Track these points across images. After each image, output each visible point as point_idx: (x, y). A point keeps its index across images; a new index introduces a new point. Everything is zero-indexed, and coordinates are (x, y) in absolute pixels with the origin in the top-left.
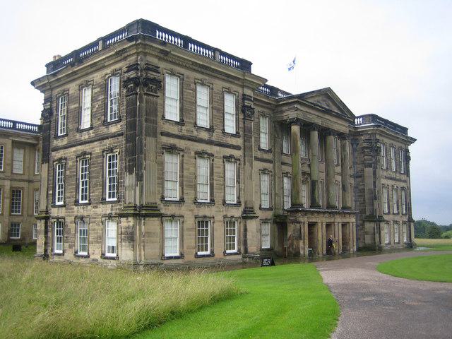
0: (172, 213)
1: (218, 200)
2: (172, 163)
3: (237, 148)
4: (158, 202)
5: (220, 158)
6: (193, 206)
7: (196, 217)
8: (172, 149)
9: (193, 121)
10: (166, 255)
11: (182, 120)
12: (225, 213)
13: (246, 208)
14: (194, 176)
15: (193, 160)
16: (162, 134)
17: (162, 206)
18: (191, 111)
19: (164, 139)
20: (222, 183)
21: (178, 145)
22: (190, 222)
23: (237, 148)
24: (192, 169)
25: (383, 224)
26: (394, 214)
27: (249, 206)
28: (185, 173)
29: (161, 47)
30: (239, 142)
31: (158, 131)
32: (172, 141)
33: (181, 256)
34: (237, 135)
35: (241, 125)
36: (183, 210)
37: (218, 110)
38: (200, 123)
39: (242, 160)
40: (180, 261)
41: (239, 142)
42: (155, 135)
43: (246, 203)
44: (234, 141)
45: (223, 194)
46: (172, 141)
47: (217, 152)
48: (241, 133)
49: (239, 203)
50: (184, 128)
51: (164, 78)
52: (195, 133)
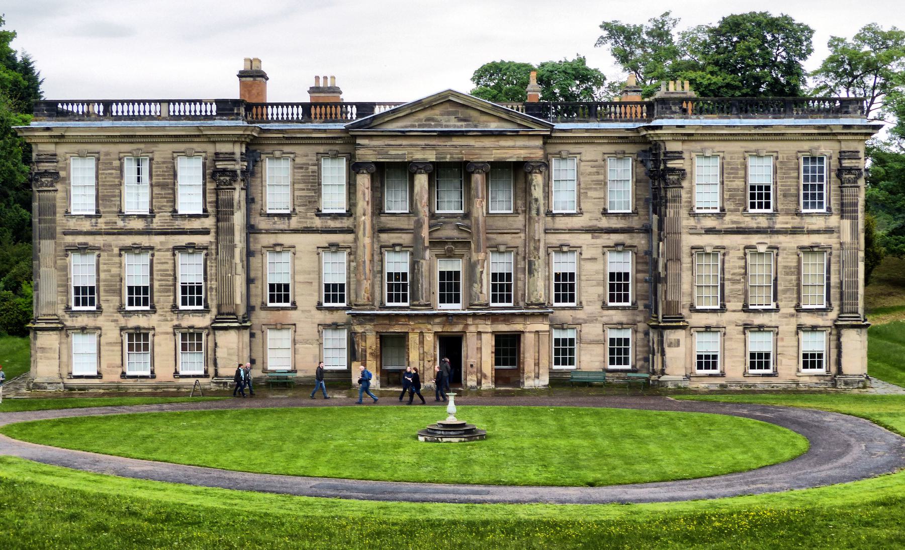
0: (83, 324)
3: (206, 232)
4: (61, 312)
5: (168, 250)
6: (119, 316)
7: (122, 329)
8: (83, 249)
9: (116, 209)
10: (75, 373)
11: (98, 211)
12: (176, 323)
13: (219, 313)
14: (118, 279)
15: (117, 259)
16: (65, 234)
17: (67, 317)
18: (114, 196)
19: (69, 239)
20: (171, 283)
21: (91, 243)
23: (206, 232)
24: (115, 270)
25: (670, 336)
26: (746, 309)
27: (225, 310)
28: (103, 276)
29: (47, 133)
31: (59, 229)
32: (81, 239)
33: (99, 376)
34: (205, 214)
35: (211, 198)
36: (100, 321)
37: (163, 186)
38: (128, 209)
39: (214, 247)
40: (97, 381)
41: (209, 223)
42: (52, 236)
43: (219, 307)
44: (196, 224)
45: (172, 298)
46: (81, 239)
47: (161, 243)
48: (209, 209)
50: (100, 220)
51: (66, 168)
52: (120, 224)
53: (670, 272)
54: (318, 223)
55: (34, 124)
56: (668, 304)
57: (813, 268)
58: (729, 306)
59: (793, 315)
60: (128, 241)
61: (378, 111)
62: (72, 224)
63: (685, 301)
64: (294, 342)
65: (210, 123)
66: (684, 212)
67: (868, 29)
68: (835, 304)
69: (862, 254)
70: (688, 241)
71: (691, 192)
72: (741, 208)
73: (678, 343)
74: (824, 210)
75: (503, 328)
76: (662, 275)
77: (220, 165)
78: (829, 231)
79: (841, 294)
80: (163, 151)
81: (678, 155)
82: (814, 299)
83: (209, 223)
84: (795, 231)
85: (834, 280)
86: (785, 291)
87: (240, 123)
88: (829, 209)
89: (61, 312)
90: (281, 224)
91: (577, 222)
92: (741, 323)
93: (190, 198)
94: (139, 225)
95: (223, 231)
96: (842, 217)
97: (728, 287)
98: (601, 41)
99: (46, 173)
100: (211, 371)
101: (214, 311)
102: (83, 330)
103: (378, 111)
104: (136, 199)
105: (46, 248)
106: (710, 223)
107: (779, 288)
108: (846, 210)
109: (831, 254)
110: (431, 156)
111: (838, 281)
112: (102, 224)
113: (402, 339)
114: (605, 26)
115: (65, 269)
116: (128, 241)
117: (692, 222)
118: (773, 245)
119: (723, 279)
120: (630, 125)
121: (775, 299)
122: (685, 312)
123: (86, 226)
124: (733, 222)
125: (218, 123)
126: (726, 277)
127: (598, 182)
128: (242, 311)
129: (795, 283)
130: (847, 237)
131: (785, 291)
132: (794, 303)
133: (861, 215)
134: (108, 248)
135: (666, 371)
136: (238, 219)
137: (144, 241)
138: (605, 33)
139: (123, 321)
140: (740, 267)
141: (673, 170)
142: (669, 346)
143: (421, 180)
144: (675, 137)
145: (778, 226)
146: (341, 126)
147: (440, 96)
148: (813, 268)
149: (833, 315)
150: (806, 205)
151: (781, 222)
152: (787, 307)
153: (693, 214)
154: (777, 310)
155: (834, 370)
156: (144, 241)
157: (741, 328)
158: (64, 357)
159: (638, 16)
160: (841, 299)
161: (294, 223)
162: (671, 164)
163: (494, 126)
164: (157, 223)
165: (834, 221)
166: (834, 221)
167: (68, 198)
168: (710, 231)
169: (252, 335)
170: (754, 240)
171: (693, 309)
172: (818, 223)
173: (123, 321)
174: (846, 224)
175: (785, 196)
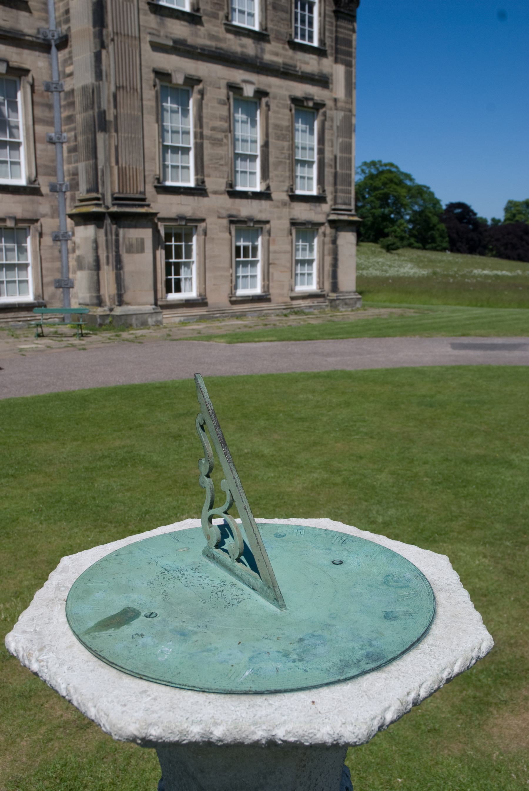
26: (234, 194)
53: (123, 111)
58: (210, 184)
59: (284, 204)
63: (153, 169)
68: (329, 189)
72: (221, 14)
74: (316, 43)
76: (110, 117)
78: (323, 81)
79: (335, 175)
84: (286, 73)
85: (328, 156)
86: (279, 163)
88: (322, 41)
92: (224, 213)
96: (336, 61)
97: (208, 150)
106: (179, 30)
107: (272, 160)
109: (324, 114)
111: (332, 157)
117: (151, 20)
118: (262, 87)
119: (199, 136)
121: (265, 175)
122: (150, 191)
124: (212, 37)
126: (206, 132)
129: (286, 152)
131: (279, 163)
132: (286, 186)
135: (127, 297)
140: (221, 119)
142: (129, 251)
145: (268, 57)
152: (280, 195)
155: (327, 286)
157: (225, 222)
160: (335, 184)
168: (180, 48)
170: (238, 76)
175: (274, 8)
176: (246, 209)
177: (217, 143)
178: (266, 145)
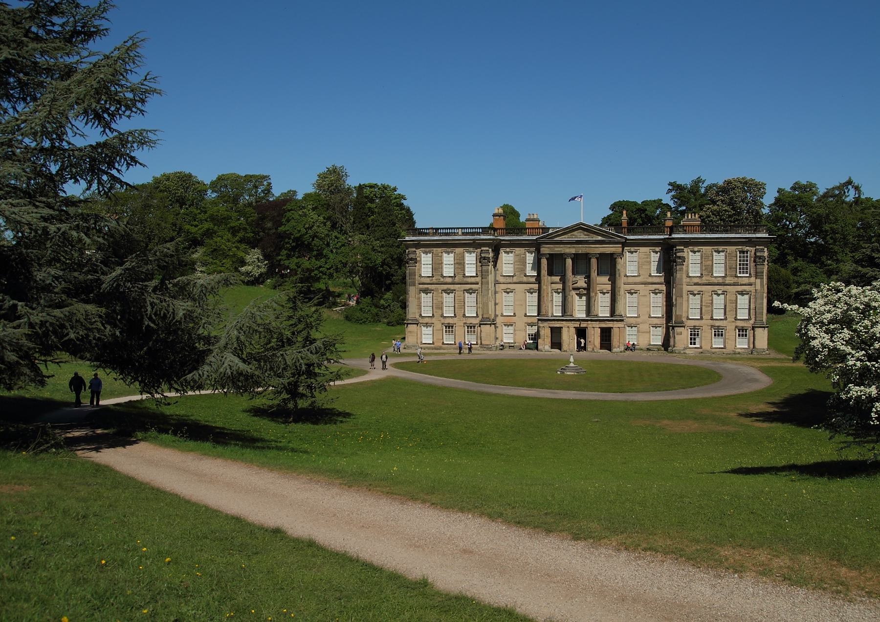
1: (460, 313)
2: (426, 299)
4: (417, 317)
8: (426, 291)
19: (421, 286)
22: (438, 326)
24: (440, 299)
27: (485, 316)
30: (478, 279)
33: (433, 343)
34: (477, 276)
36: (433, 320)
37: (459, 264)
44: (473, 280)
46: (426, 286)
49: (477, 316)
51: (420, 257)
52: (442, 280)
54: (525, 279)
55: (407, 238)
56: (676, 316)
57: (743, 301)
60: (445, 287)
61: (550, 231)
62: (423, 280)
63: (684, 315)
64: (515, 330)
65: (478, 237)
66: (684, 276)
67: (796, 183)
68: (753, 317)
69: (765, 295)
70: (686, 288)
71: (688, 266)
73: (681, 334)
75: (604, 325)
77: (483, 255)
80: (459, 250)
81: (682, 251)
82: (743, 314)
83: (478, 279)
84: (734, 284)
85: (752, 306)
87: (492, 237)
89: (417, 317)
90: (509, 280)
91: (638, 280)
93: (471, 270)
94: (450, 280)
95: (485, 283)
98: (670, 191)
99: (411, 259)
100: (479, 342)
101: (480, 317)
102: (427, 325)
103: (550, 231)
104: (448, 271)
105: (412, 291)
108: (758, 275)
110: (573, 251)
112: (434, 280)
113: (560, 329)
114: (670, 184)
115: (419, 299)
116: (445, 287)
117: (688, 280)
120: (662, 237)
122: (684, 320)
123: (428, 280)
125: (483, 237)
127: (647, 262)
128: (493, 317)
130: (758, 287)
133: (765, 277)
134: (437, 290)
136: (491, 278)
137: (452, 287)
138: (671, 187)
139: (443, 321)
141: (680, 257)
143: (569, 262)
144: (681, 244)
146: (534, 238)
147: (577, 225)
148: (743, 301)
149: (752, 322)
150: (740, 273)
151: (729, 280)
152: (730, 318)
153: (688, 276)
154: (726, 319)
155: (752, 346)
156: (452, 287)
158: (419, 336)
159: (686, 180)
161: (515, 279)
162: (678, 254)
163: (600, 238)
164: (457, 280)
165: (753, 279)
166: (753, 279)
167: (420, 269)
168: (696, 284)
169: (496, 327)
170: (716, 288)
171: (688, 319)
172: (746, 281)
173: (443, 321)
174: (758, 281)
176: (717, 323)
177: (707, 306)
178: (725, 306)
